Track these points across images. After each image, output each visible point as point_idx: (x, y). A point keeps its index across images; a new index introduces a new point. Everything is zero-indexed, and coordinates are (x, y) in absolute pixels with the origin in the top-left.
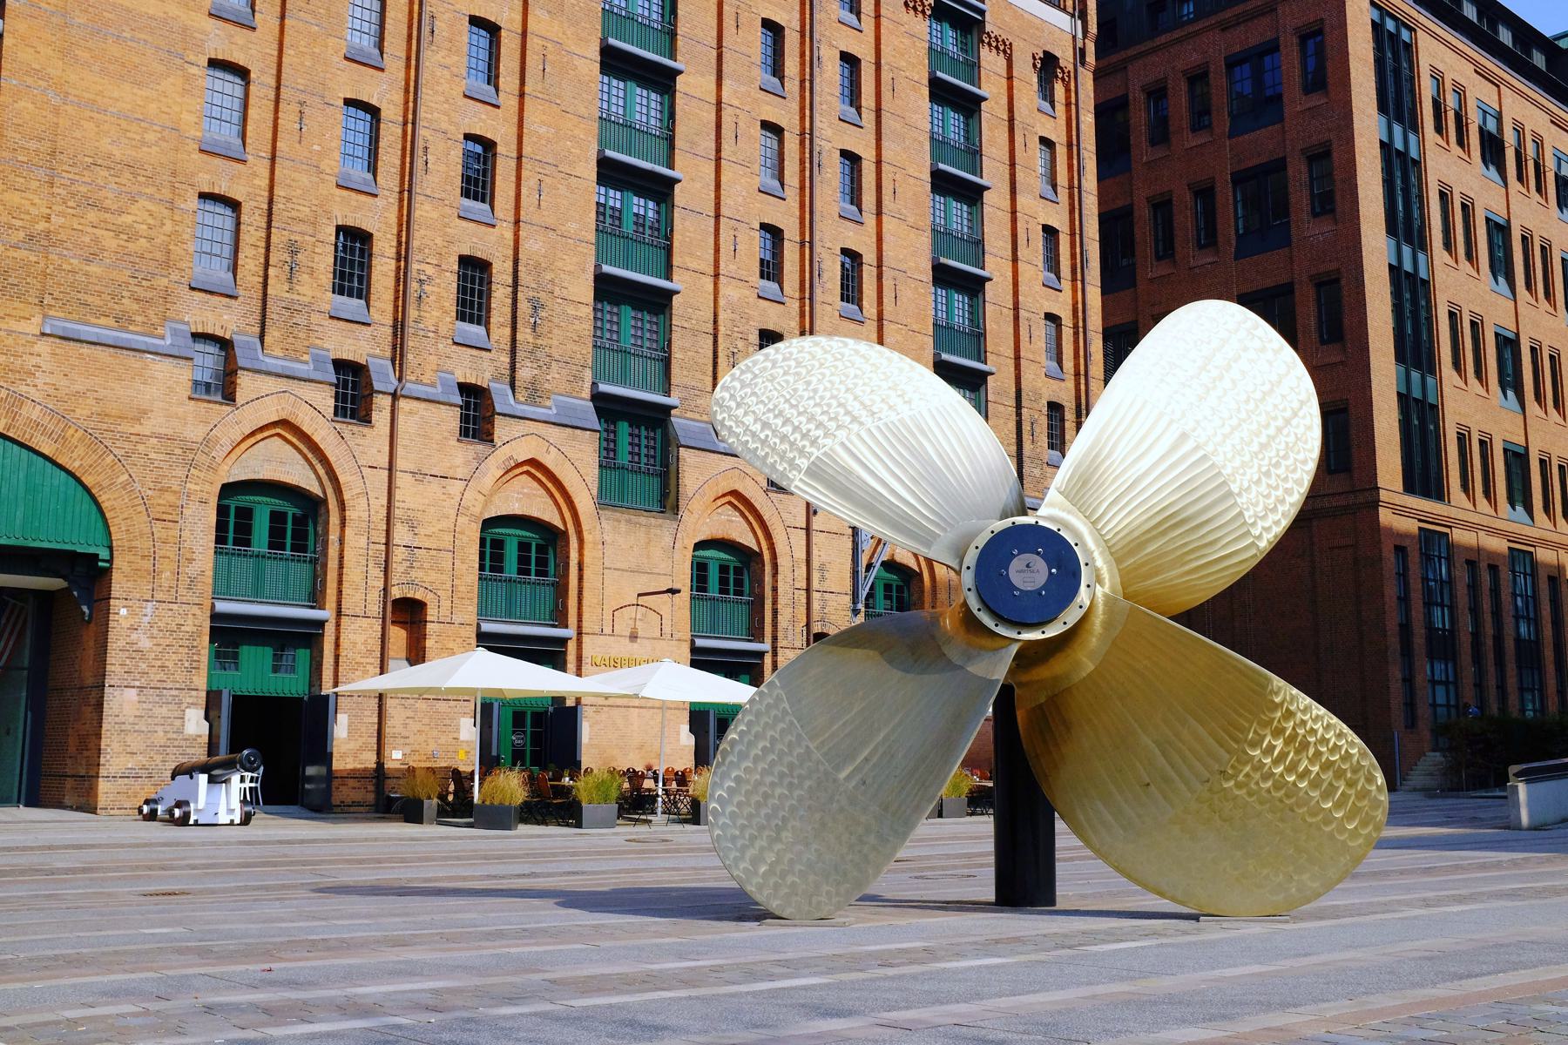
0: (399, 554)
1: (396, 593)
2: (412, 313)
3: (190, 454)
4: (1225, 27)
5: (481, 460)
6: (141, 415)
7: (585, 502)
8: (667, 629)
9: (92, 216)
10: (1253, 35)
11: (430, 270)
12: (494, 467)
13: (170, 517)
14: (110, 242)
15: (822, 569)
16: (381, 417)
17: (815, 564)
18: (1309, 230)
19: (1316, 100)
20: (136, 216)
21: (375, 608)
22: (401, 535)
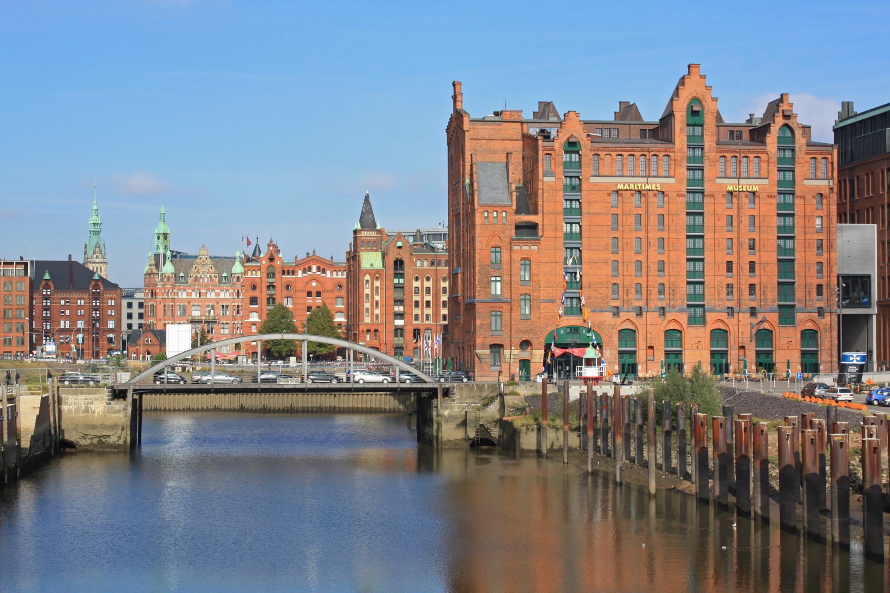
0: (648, 339)
1: (648, 345)
2: (649, 297)
3: (613, 327)
5: (663, 321)
6: (605, 322)
7: (685, 326)
8: (703, 347)
9: (596, 292)
11: (652, 288)
12: (666, 322)
13: (610, 337)
14: (599, 295)
15: (742, 333)
16: (644, 316)
17: (740, 331)
20: (602, 291)
21: (645, 348)
22: (649, 335)
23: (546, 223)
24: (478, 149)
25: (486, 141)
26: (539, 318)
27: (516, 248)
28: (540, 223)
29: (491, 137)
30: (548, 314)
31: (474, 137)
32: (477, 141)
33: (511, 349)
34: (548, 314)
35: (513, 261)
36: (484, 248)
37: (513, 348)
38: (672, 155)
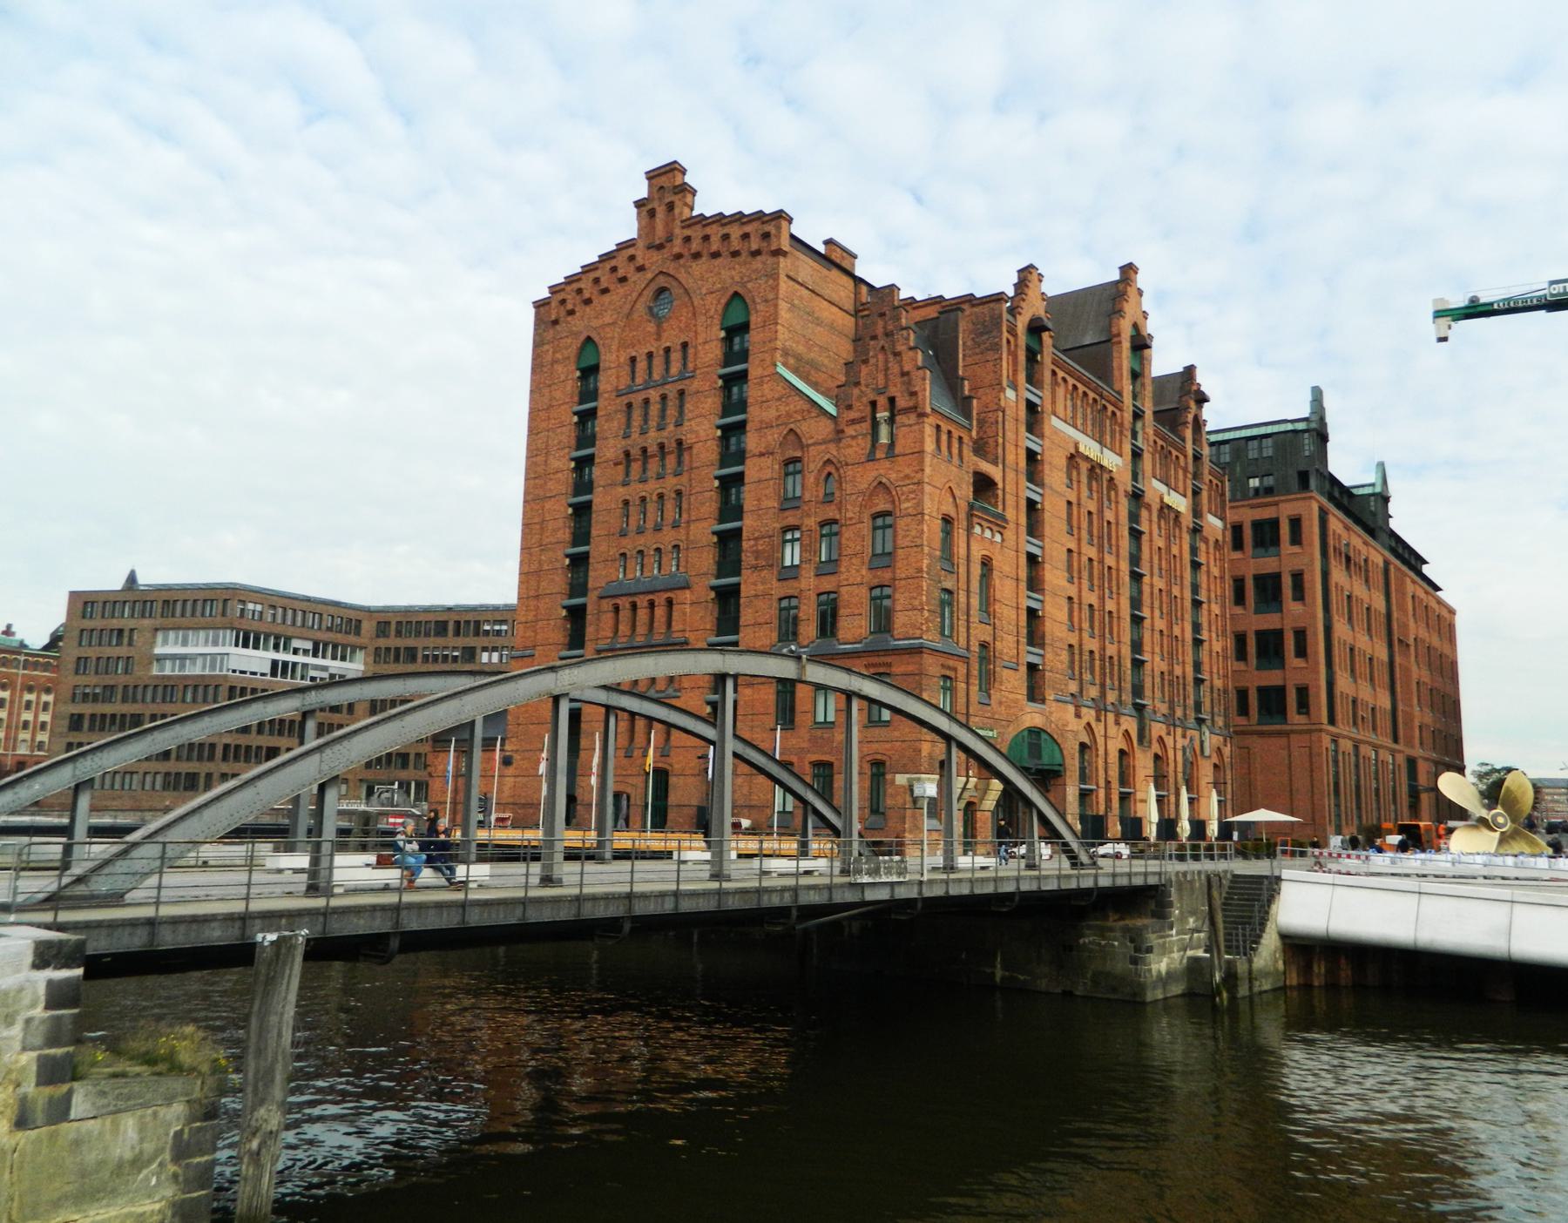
4: (1252, 507)
10: (1267, 514)
18: (1292, 607)
19: (1296, 549)
23: (1007, 487)
24: (796, 302)
25: (807, 292)
26: (1000, 703)
27: (977, 530)
28: (1000, 485)
29: (817, 289)
30: (1011, 696)
31: (791, 274)
32: (797, 286)
33: (968, 776)
34: (1011, 696)
35: (972, 558)
36: (934, 514)
37: (971, 773)
38: (1118, 413)
